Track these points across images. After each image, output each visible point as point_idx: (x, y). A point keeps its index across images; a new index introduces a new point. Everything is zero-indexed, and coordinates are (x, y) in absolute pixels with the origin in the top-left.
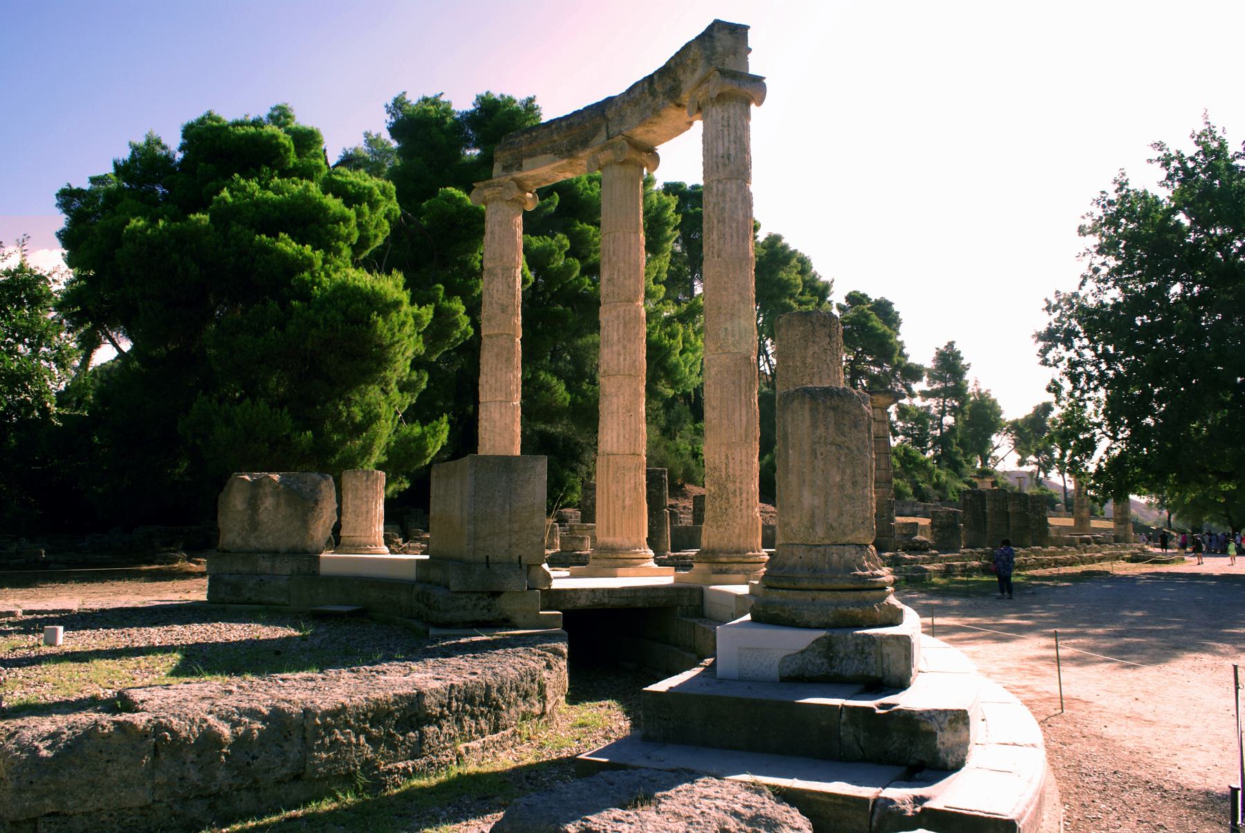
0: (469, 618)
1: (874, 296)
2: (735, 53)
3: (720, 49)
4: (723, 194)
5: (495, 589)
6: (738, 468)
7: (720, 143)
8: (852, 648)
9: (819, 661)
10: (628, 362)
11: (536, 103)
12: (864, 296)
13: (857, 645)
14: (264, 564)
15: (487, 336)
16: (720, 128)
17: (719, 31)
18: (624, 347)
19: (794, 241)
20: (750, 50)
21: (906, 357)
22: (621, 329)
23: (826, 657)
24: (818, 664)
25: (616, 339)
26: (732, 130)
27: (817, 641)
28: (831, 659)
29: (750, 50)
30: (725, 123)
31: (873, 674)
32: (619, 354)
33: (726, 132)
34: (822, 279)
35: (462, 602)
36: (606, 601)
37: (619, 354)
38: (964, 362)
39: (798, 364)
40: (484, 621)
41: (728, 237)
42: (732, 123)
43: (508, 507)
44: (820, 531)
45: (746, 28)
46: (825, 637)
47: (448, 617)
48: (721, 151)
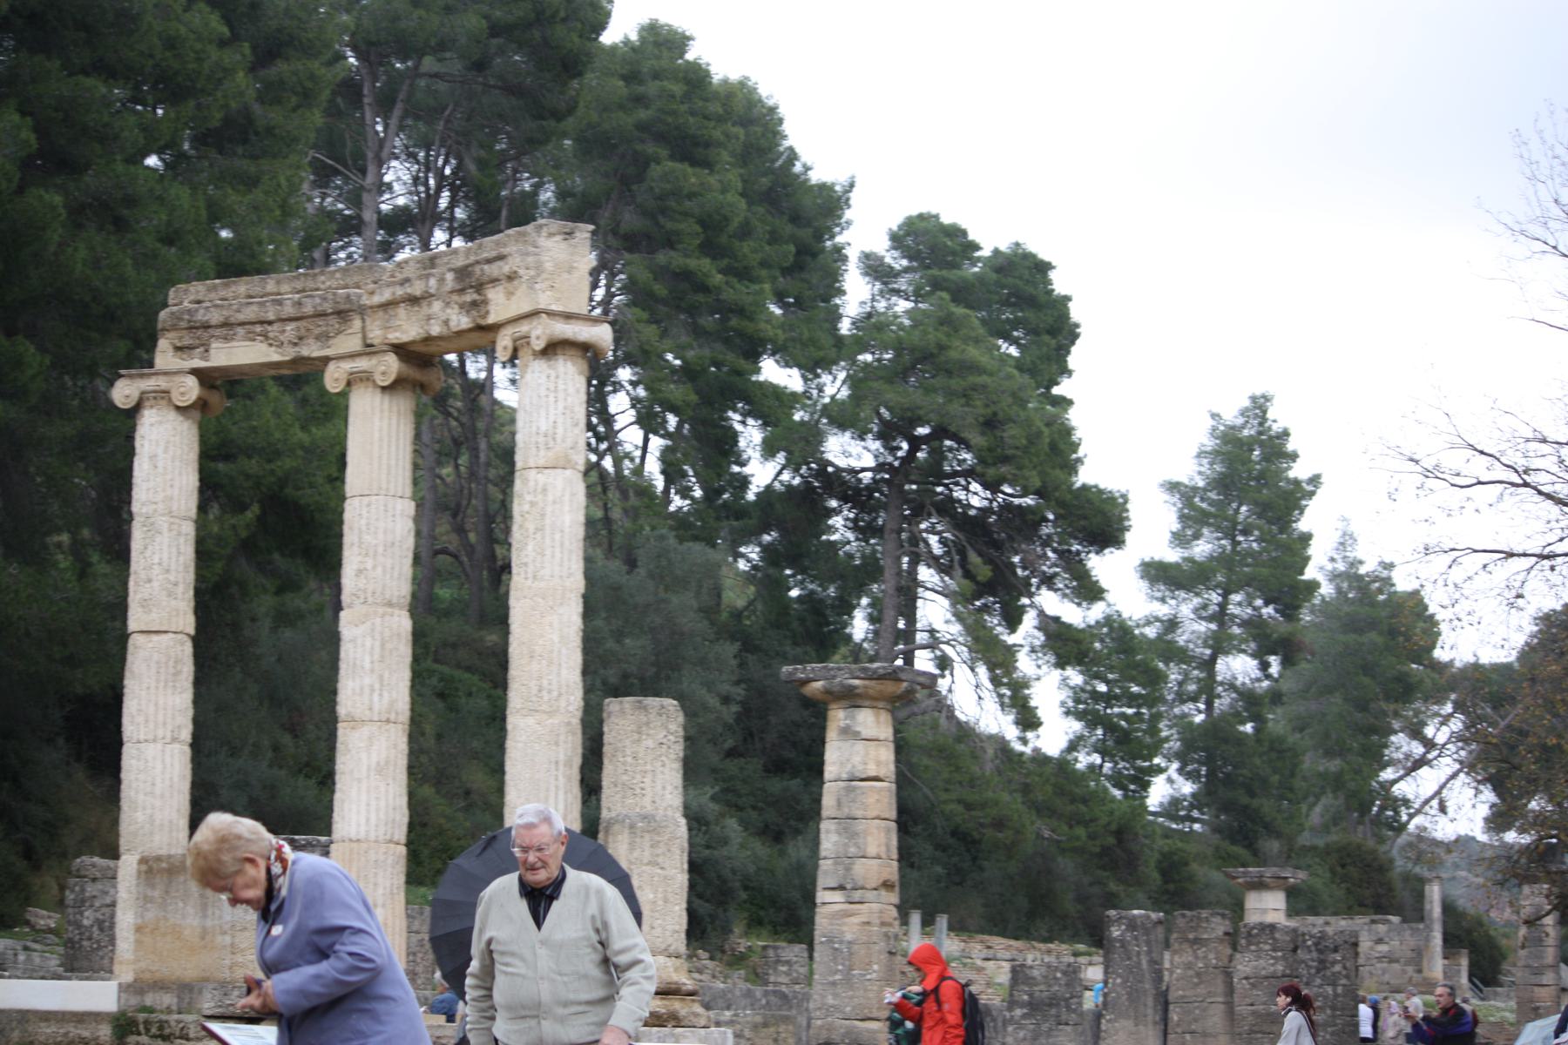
1: (991, 237)
3: (548, 266)
4: (545, 490)
7: (543, 413)
12: (957, 232)
16: (543, 392)
18: (381, 677)
19: (720, 55)
21: (1072, 467)
22: (377, 650)
25: (367, 665)
32: (372, 690)
33: (552, 399)
34: (815, 177)
37: (372, 690)
38: (1299, 471)
39: (629, 759)
41: (548, 552)
42: (561, 387)
48: (543, 428)
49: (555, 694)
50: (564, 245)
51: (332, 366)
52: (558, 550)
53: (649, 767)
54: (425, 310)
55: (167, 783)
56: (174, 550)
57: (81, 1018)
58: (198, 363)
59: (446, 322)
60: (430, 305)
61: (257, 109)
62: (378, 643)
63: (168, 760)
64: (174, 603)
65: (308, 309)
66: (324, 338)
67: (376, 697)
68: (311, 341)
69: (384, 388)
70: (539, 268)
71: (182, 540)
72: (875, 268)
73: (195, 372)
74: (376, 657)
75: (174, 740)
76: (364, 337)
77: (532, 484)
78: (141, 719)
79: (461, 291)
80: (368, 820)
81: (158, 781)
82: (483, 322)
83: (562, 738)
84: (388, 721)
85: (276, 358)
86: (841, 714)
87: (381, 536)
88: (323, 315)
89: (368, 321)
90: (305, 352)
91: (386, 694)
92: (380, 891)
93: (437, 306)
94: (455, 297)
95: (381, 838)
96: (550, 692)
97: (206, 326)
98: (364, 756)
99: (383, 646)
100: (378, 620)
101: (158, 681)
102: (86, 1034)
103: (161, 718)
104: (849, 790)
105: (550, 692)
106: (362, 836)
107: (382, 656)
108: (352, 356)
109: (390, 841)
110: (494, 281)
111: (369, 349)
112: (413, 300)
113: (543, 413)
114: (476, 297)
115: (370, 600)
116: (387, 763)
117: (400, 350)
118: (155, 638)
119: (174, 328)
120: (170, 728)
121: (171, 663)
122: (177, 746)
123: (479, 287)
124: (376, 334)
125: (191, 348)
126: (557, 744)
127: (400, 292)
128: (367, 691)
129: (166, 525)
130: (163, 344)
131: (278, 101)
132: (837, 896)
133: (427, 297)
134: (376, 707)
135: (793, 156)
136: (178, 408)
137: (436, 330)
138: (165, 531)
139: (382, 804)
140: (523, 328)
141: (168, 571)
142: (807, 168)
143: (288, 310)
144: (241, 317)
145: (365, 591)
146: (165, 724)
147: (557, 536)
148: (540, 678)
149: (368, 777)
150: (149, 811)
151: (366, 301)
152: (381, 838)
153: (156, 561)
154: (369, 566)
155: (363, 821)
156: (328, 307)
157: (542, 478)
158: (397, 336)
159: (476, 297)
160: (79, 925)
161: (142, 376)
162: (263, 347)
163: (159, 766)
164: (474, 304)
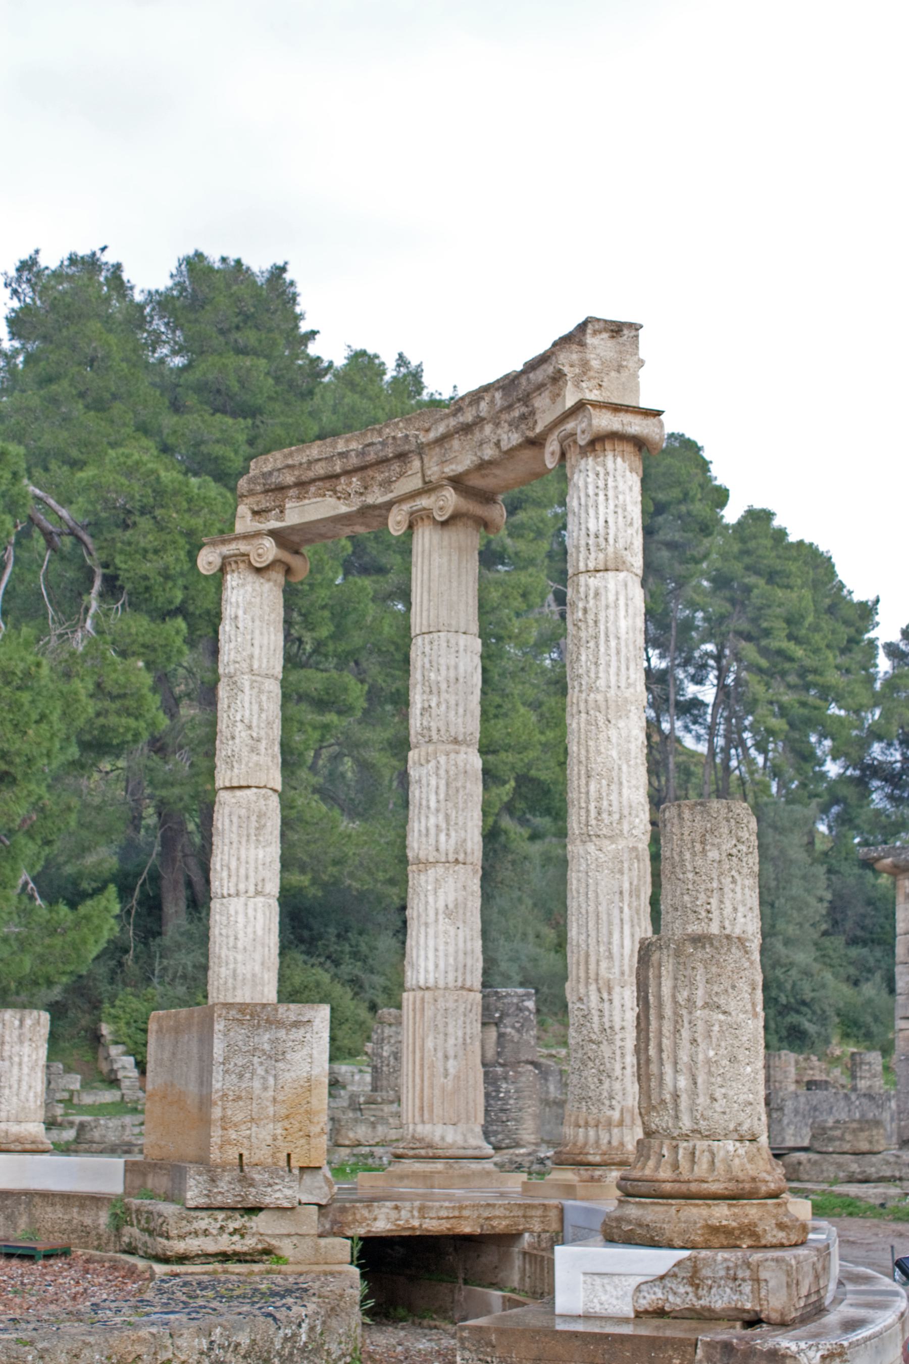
0: (211, 1246)
2: (619, 368)
3: (595, 364)
4: (597, 594)
5: (251, 1201)
6: (617, 1019)
8: (722, 1273)
9: (682, 1290)
10: (452, 842)
11: (288, 276)
13: (728, 1268)
15: (226, 788)
17: (595, 332)
18: (447, 816)
20: (641, 363)
23: (692, 1284)
24: (680, 1297)
25: (433, 804)
26: (611, 494)
27: (678, 1264)
28: (697, 1287)
29: (641, 363)
30: (601, 484)
31: (748, 1306)
33: (601, 497)
34: (857, 597)
35: (202, 1224)
36: (416, 1223)
39: (690, 876)
40: (236, 1253)
41: (602, 661)
43: (271, 1081)
44: (686, 1123)
45: (636, 327)
46: (689, 1259)
47: (180, 1247)
49: (616, 817)
50: (610, 343)
51: (395, 509)
52: (614, 658)
53: (715, 885)
54: (477, 436)
55: (251, 936)
56: (255, 707)
58: (274, 524)
59: (498, 444)
60: (482, 429)
61: (508, 541)
62: (442, 783)
63: (251, 912)
64: (255, 758)
65: (372, 457)
66: (387, 484)
67: (443, 837)
68: (376, 489)
69: (444, 524)
70: (585, 365)
71: (264, 698)
72: (892, 650)
73: (272, 533)
74: (442, 796)
75: (258, 893)
76: (423, 476)
77: (582, 589)
78: (225, 874)
79: (509, 408)
80: (437, 966)
81: (241, 935)
82: (531, 434)
83: (626, 865)
84: (457, 861)
85: (343, 509)
87: (443, 672)
88: (385, 461)
89: (426, 460)
90: (370, 500)
91: (453, 834)
92: (451, 1041)
93: (488, 429)
94: (505, 416)
95: (451, 984)
96: (610, 814)
97: (281, 488)
98: (431, 899)
99: (448, 785)
100: (442, 759)
101: (239, 835)
102: (88, 1221)
103: (242, 871)
105: (610, 814)
106: (431, 983)
107: (447, 794)
109: (462, 988)
110: (540, 387)
111: (429, 488)
112: (466, 429)
113: (592, 512)
114: (524, 409)
115: (435, 737)
116: (456, 906)
117: (457, 482)
118: (238, 793)
119: (252, 493)
120: (252, 880)
121: (254, 818)
122: (260, 900)
123: (526, 399)
124: (434, 471)
125: (267, 511)
126: (621, 872)
127: (452, 422)
128: (433, 831)
129: (247, 685)
130: (243, 510)
131: (521, 536)
133: (479, 421)
134: (442, 847)
135: (841, 586)
136: (258, 571)
137: (489, 453)
138: (247, 689)
139: (451, 949)
140: (570, 426)
141: (250, 727)
142: (850, 593)
143: (354, 461)
144: (311, 475)
145: (429, 729)
146: (247, 877)
147: (613, 643)
148: (599, 799)
149: (436, 921)
150: (231, 966)
151: (423, 439)
152: (451, 984)
153: (238, 718)
154: (433, 704)
155: (431, 967)
156: (390, 452)
157: (593, 582)
158: (452, 469)
159: (524, 409)
160: (381, 1057)
161: (224, 542)
162: (331, 500)
163: (241, 919)
164: (523, 417)
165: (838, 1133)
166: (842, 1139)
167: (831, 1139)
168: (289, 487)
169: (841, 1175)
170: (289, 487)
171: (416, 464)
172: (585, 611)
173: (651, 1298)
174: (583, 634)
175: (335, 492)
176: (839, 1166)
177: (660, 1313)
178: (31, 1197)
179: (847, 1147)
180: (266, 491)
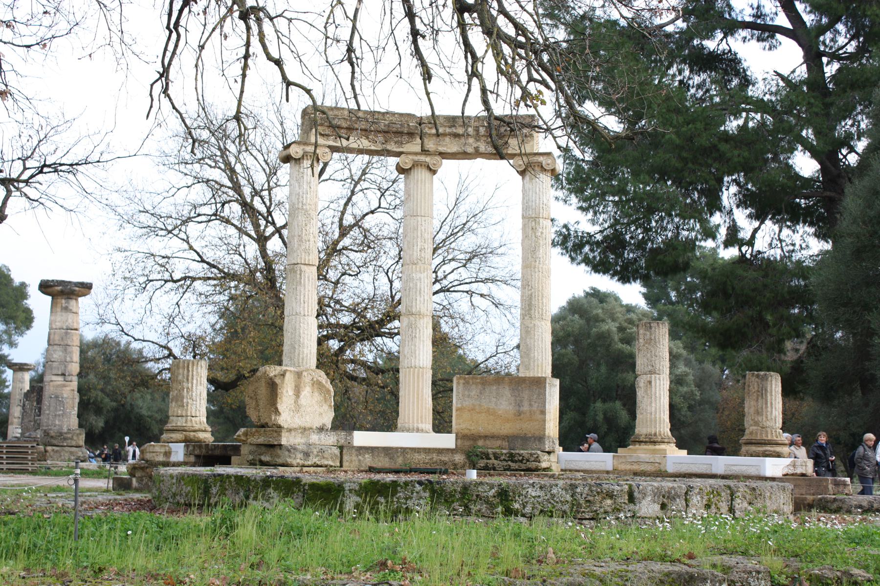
14: (314, 438)
54: (463, 140)
57: (440, 451)
85: (373, 148)
86: (63, 301)
89: (426, 140)
93: (471, 140)
102: (446, 459)
104: (66, 333)
108: (416, 154)
125: (328, 135)
132: (60, 378)
140: (541, 159)
165: (69, 436)
166: (72, 439)
167: (65, 439)
168: (342, 128)
169: (72, 458)
170: (342, 128)
171: (418, 140)
172: (542, 233)
173: (785, 473)
174: (541, 242)
175: (368, 138)
176: (71, 453)
177: (787, 475)
178: (404, 450)
179: (74, 443)
180: (329, 127)
